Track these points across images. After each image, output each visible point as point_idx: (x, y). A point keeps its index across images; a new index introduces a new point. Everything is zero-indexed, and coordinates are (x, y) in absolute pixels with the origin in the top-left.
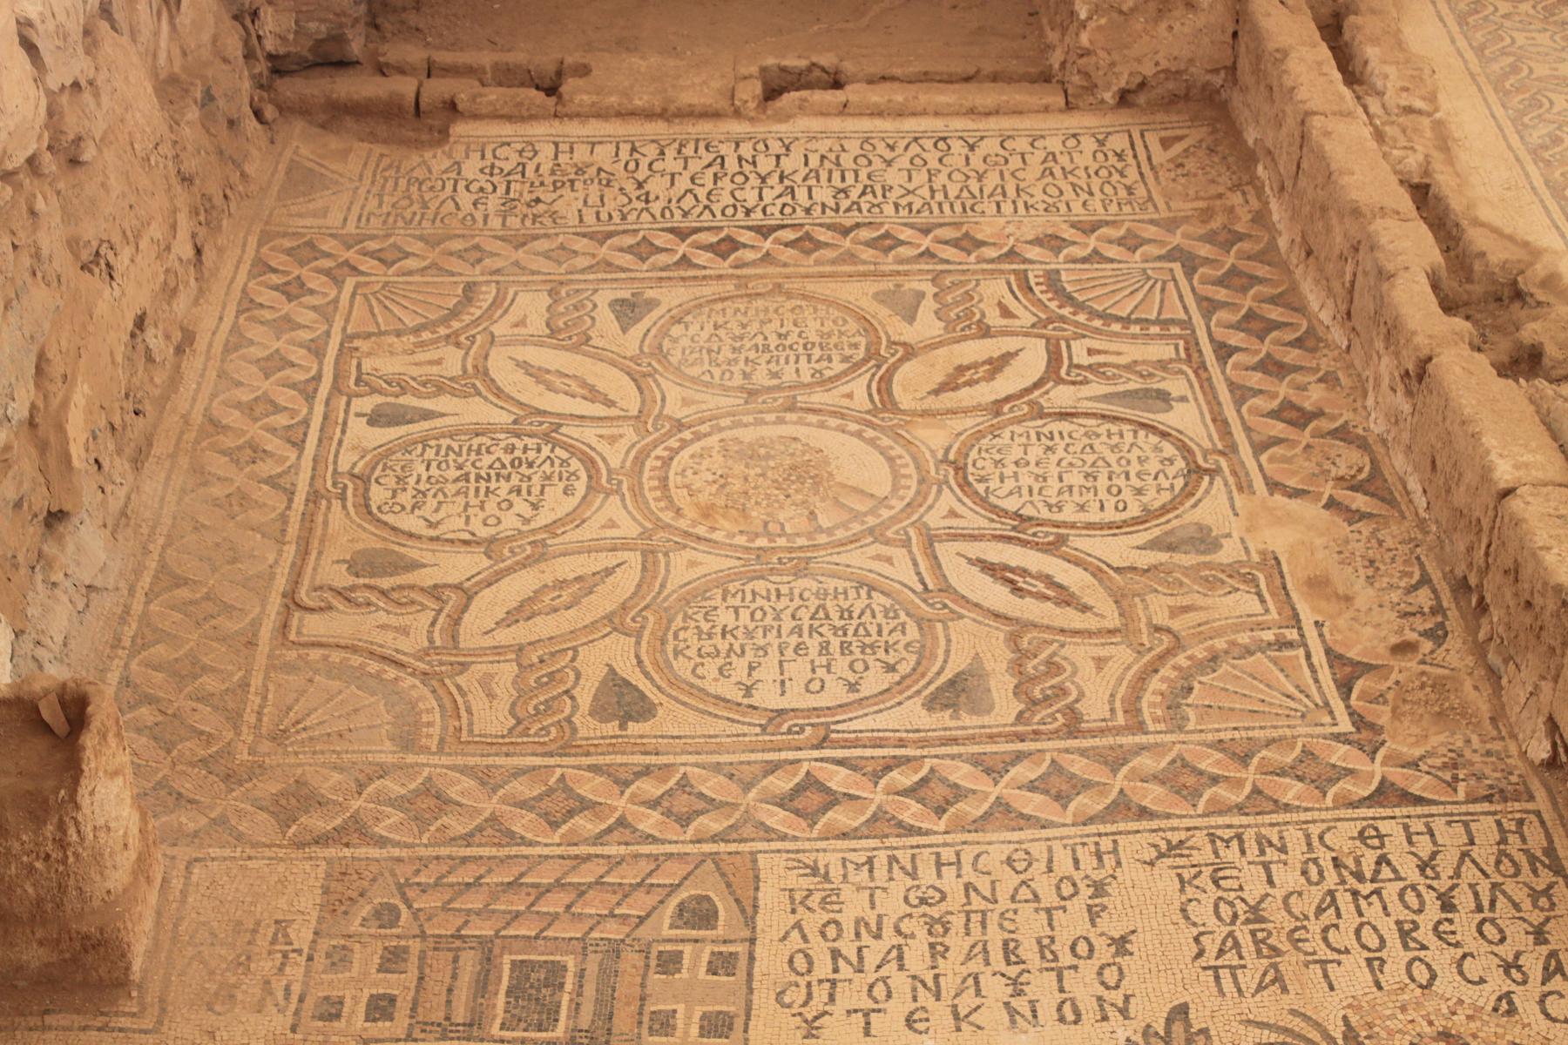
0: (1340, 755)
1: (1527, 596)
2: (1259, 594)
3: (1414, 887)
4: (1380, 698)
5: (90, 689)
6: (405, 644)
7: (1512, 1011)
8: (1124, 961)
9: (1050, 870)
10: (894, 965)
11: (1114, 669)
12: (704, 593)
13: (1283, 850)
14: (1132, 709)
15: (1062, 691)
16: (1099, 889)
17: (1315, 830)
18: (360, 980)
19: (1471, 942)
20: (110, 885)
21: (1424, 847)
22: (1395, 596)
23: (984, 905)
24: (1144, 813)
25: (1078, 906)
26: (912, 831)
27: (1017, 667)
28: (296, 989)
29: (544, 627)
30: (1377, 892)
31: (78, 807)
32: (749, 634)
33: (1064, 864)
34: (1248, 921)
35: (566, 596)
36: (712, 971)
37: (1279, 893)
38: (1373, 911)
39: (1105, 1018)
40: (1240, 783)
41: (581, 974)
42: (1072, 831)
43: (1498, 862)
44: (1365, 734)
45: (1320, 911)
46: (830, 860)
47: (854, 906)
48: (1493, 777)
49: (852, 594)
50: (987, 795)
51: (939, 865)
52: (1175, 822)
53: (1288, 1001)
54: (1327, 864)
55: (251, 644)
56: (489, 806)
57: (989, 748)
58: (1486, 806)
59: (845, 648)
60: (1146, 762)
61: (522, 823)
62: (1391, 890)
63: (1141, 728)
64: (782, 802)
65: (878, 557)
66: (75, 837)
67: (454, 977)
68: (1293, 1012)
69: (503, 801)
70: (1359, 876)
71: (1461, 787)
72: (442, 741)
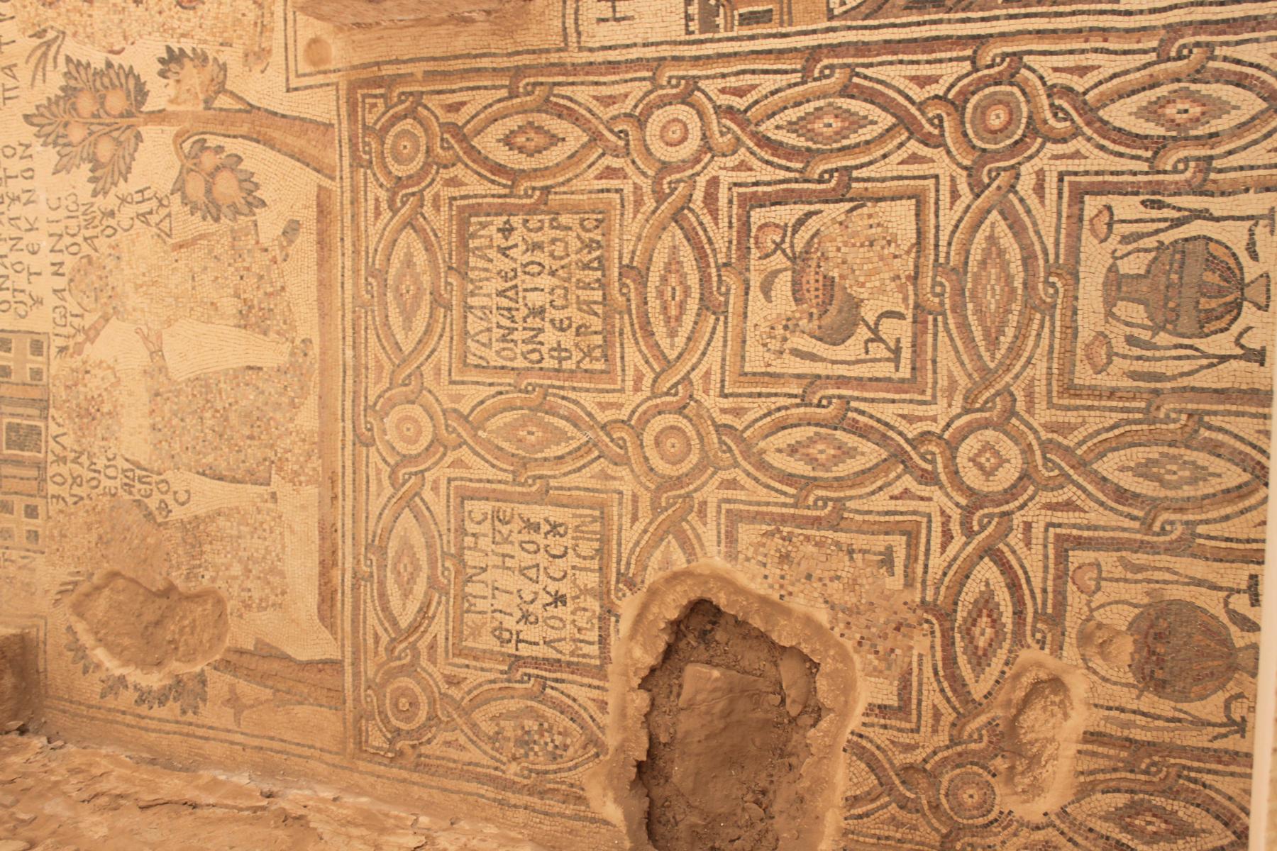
28: (23, 553)
41: (13, 415)
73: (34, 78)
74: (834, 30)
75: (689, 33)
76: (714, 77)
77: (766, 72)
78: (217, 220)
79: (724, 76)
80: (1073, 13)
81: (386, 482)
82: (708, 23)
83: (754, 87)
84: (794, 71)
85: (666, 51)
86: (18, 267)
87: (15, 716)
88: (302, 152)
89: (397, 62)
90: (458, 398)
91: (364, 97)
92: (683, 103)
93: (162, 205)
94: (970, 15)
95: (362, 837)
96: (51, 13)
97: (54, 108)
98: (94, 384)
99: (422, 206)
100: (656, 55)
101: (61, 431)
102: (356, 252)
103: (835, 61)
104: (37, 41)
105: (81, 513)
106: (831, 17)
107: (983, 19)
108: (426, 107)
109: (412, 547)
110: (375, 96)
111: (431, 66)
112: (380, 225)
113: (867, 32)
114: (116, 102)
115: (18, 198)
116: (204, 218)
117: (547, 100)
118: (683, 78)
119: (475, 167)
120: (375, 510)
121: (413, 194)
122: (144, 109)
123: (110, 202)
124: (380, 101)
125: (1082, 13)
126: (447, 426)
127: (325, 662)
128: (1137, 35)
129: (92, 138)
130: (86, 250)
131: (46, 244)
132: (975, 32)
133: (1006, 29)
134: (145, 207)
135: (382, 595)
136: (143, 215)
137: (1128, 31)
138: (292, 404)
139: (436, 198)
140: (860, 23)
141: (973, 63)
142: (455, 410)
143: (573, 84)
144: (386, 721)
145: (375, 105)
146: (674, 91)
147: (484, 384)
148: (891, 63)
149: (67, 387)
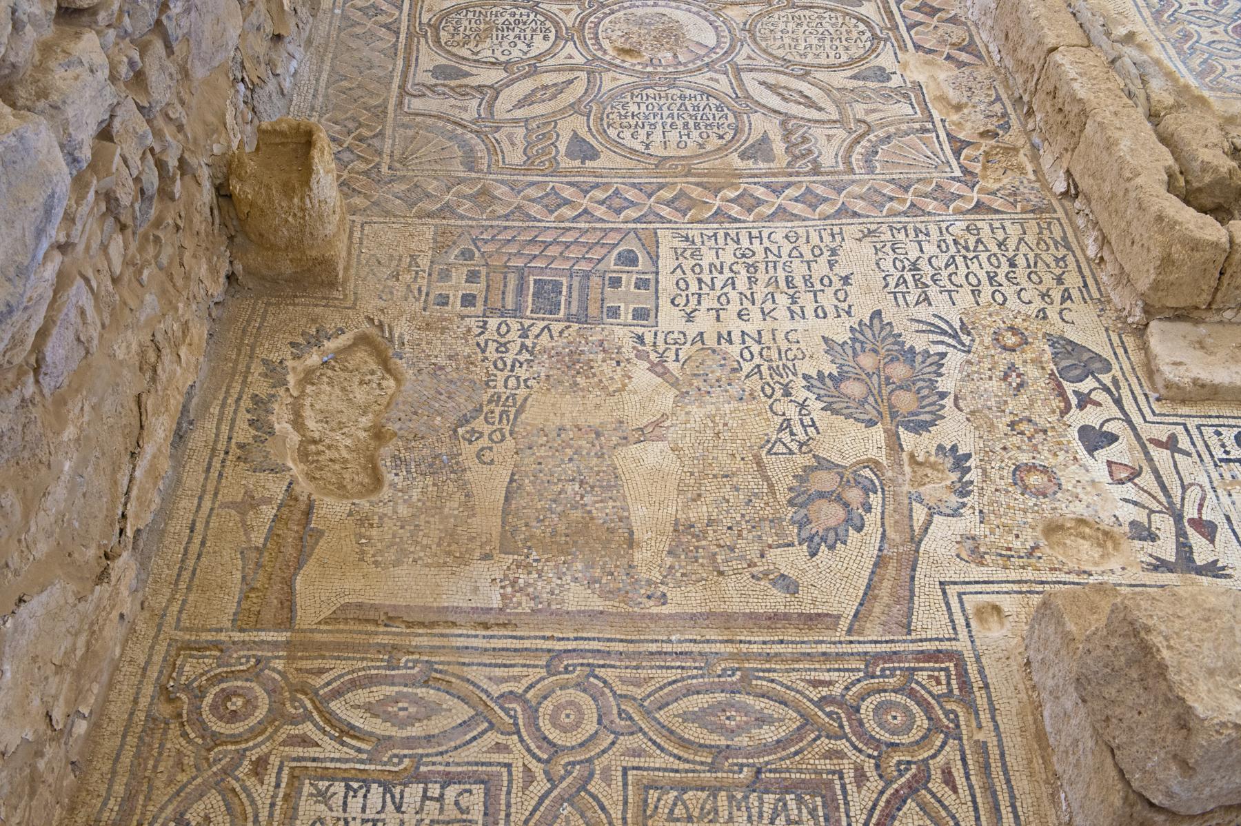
0: (955, 187)
1: (1060, 106)
2: (912, 104)
3: (995, 255)
4: (975, 160)
5: (315, 129)
6: (465, 116)
7: (1045, 317)
8: (848, 288)
9: (808, 242)
10: (730, 287)
11: (836, 142)
12: (622, 95)
13: (927, 235)
14: (847, 161)
15: (810, 151)
16: (834, 252)
17: (944, 225)
18: (457, 286)
19: (1025, 284)
20: (327, 232)
21: (1000, 235)
22: (983, 107)
23: (775, 259)
24: (855, 214)
25: (823, 261)
26: (736, 220)
27: (786, 138)
28: (424, 290)
29: (539, 109)
30: (976, 257)
31: (311, 190)
32: (646, 117)
33: (814, 238)
34: (910, 270)
35: (549, 93)
36: (637, 287)
37: (926, 257)
38: (974, 266)
39: (839, 316)
40: (905, 200)
41: (570, 287)
42: (819, 222)
43: (1038, 244)
44: (968, 178)
45: (947, 266)
46: (694, 232)
47: (708, 258)
48: (1034, 200)
49: (699, 98)
50: (774, 204)
51: (751, 238)
52: (872, 220)
53: (931, 310)
54: (951, 243)
55: (385, 112)
56: (517, 200)
57: (773, 179)
58: (1032, 215)
59: (697, 126)
60: (855, 189)
61: (535, 210)
62: (983, 257)
63: (852, 171)
64: (669, 203)
65: (712, 79)
66: (309, 206)
67: (505, 286)
68: (935, 315)
69: (524, 198)
70: (967, 249)
71: (1019, 205)
72: (489, 166)
73: (919, 321)
78: (791, 502)
81: (505, 688)
86: (723, 299)
87: (246, 269)
88: (875, 597)
89: (993, 710)
90: (607, 778)
91: (946, 669)
93: (801, 445)
95: (74, 649)
96: (988, 340)
97: (891, 340)
98: (607, 369)
99: (828, 737)
101: (555, 334)
102: (769, 657)
104: (957, 326)
105: (467, 351)
108: (944, 744)
109: (428, 718)
110: (949, 684)
111: (994, 752)
112: (801, 685)
114: (905, 401)
115: (796, 303)
116: (790, 489)
119: (882, 803)
120: (471, 673)
121: (841, 727)
122: (901, 429)
123: (800, 394)
124: (943, 689)
126: (573, 764)
127: (292, 610)
129: (864, 376)
130: (747, 367)
131: (750, 328)
134: (798, 429)
135: (371, 681)
136: (789, 426)
138: (592, 581)
139: (840, 755)
142: (592, 775)
144: (219, 679)
145: (939, 683)
147: (625, 811)
149: (601, 342)
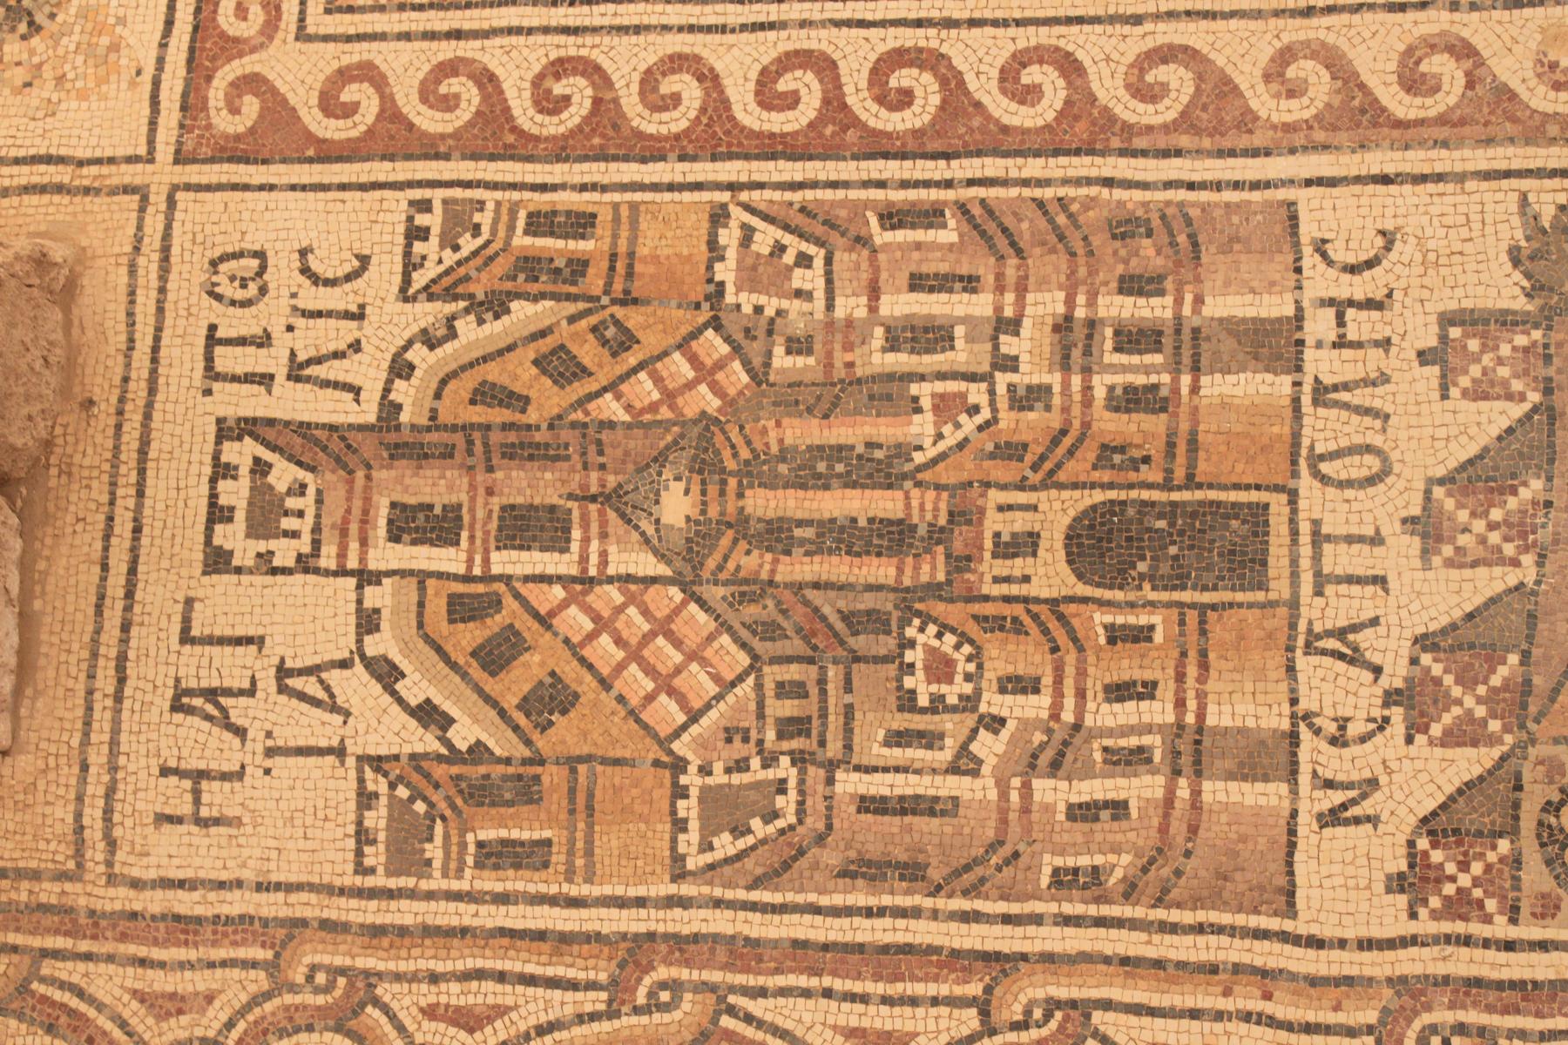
74: (683, 903)
75: (362, 869)
76: (413, 978)
77: (530, 980)
79: (434, 978)
80: (1200, 929)
82: (407, 857)
83: (501, 1011)
84: (592, 986)
85: (307, 906)
92: (338, 1029)
94: (979, 905)
100: (284, 912)
103: (685, 974)
106: (679, 876)
107: (1007, 919)
113: (756, 917)
117: (23, 989)
118: (342, 971)
125: (1219, 930)
128: (1333, 993)
132: (990, 946)
133: (1058, 947)
137: (1314, 981)
140: (741, 894)
141: (985, 1013)
143: (88, 957)
146: (320, 1000)
148: (806, 993)
